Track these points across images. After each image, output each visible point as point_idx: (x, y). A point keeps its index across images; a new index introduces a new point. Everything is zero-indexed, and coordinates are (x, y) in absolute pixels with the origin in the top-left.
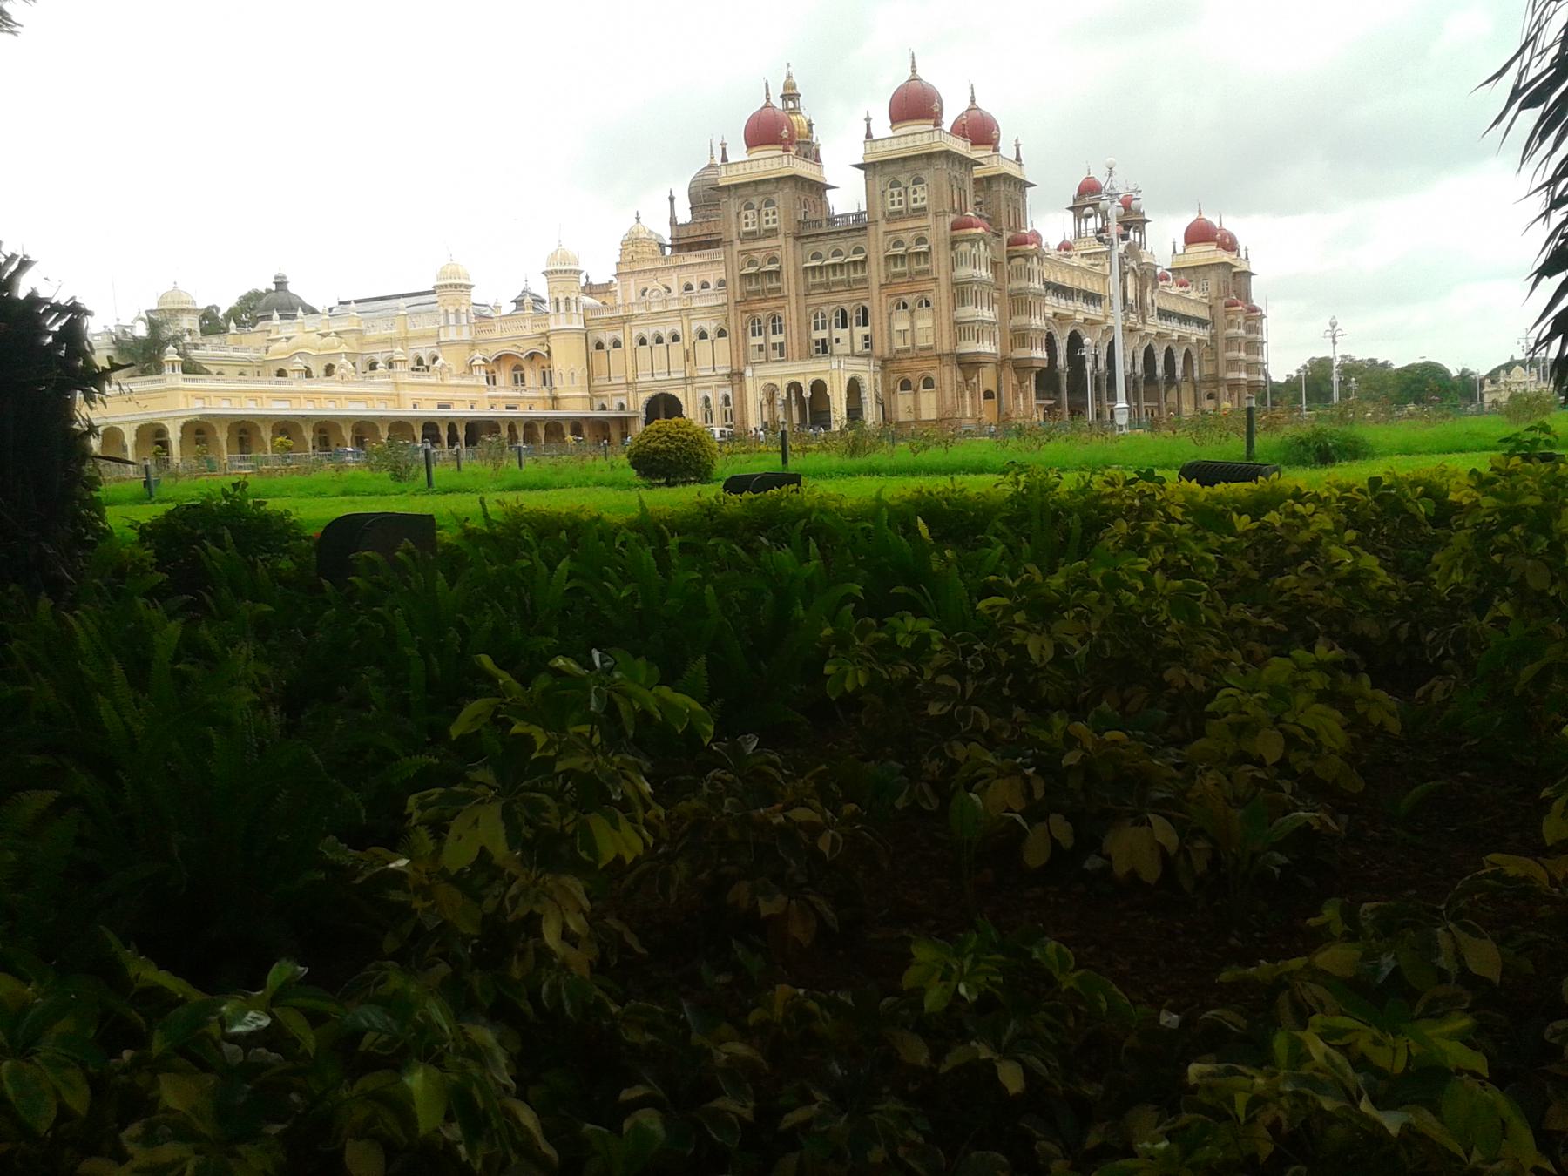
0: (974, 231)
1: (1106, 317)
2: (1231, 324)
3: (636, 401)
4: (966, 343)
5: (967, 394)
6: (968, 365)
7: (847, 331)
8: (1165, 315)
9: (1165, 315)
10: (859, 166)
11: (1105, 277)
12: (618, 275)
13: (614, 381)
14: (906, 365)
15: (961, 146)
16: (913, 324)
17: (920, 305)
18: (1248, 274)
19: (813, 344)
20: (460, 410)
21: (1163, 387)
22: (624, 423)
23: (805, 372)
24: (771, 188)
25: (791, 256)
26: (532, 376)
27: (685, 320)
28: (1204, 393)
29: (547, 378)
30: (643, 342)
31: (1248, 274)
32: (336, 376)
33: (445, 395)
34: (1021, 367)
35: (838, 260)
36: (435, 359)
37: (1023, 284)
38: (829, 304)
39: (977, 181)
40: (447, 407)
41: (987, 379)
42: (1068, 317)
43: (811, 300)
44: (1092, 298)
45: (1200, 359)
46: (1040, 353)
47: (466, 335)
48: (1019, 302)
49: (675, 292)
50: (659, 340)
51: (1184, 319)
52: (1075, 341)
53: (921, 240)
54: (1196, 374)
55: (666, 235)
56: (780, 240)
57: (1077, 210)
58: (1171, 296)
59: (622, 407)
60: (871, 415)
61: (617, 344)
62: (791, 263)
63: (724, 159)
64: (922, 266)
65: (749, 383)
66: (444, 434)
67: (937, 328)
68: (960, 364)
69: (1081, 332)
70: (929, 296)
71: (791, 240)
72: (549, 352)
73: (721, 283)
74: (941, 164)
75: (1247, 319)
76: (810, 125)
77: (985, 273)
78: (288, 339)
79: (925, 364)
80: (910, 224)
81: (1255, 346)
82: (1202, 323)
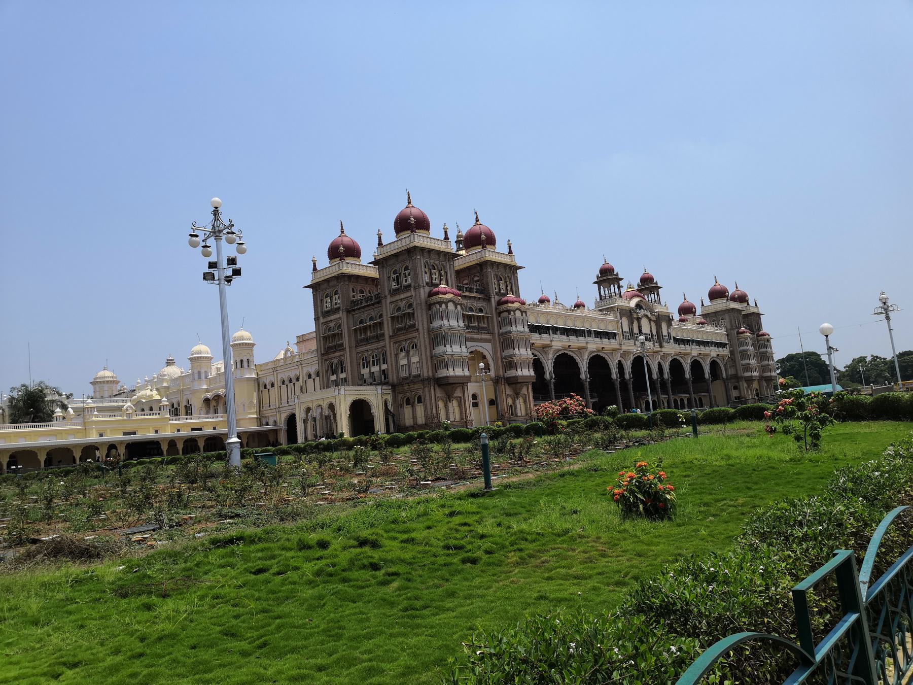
0: (441, 296)
1: (620, 345)
2: (741, 344)
5: (450, 405)
6: (449, 387)
9: (678, 341)
16: (409, 362)
18: (759, 315)
22: (275, 432)
28: (731, 386)
31: (759, 315)
45: (725, 366)
54: (724, 375)
59: (275, 423)
61: (273, 385)
62: (346, 327)
67: (421, 362)
68: (439, 386)
71: (345, 313)
80: (402, 296)
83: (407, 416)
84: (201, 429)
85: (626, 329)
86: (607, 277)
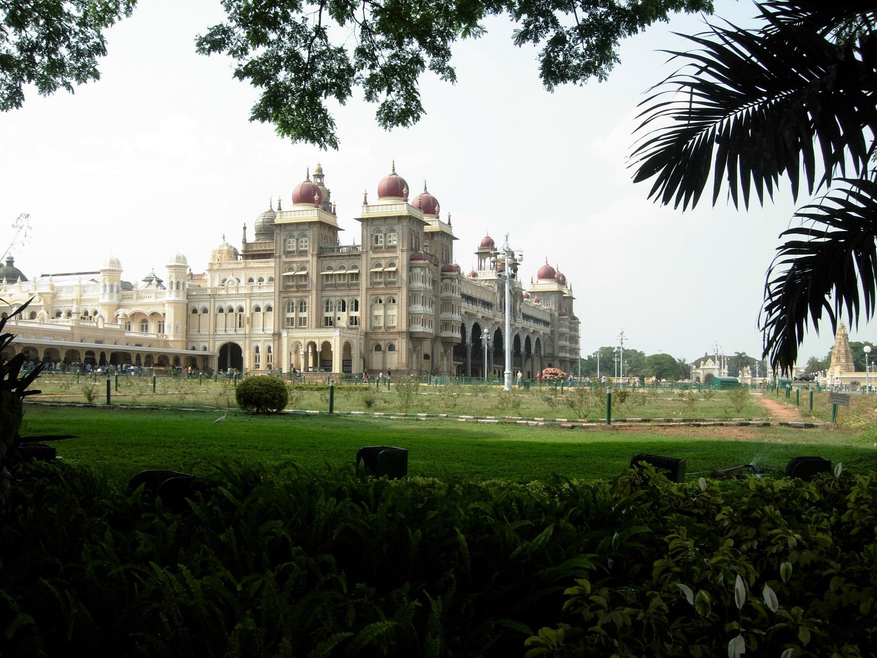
0: (422, 262)
1: (494, 316)
2: (560, 326)
3: (214, 345)
4: (416, 326)
7: (345, 313)
8: (526, 317)
9: (526, 317)
10: (359, 220)
11: (494, 294)
12: (210, 270)
13: (201, 332)
14: (380, 336)
15: (418, 214)
16: (385, 313)
17: (390, 302)
19: (323, 319)
20: (108, 346)
21: (524, 358)
22: (206, 358)
23: (319, 336)
24: (306, 227)
25: (315, 266)
26: (153, 327)
27: (248, 300)
29: (161, 328)
30: (221, 311)
31: (571, 298)
32: (36, 320)
33: (99, 335)
34: (446, 342)
35: (343, 272)
36: (96, 313)
37: (448, 294)
38: (336, 296)
39: (426, 233)
40: (101, 342)
41: (426, 348)
42: (473, 315)
43: (326, 294)
44: (487, 305)
46: (457, 335)
47: (115, 300)
48: (446, 304)
49: (243, 283)
50: (231, 310)
51: (537, 320)
52: (477, 330)
53: (392, 265)
54: (542, 353)
55: (240, 249)
56: (309, 258)
57: (482, 255)
58: (531, 305)
59: (205, 349)
60: (356, 367)
61: (205, 311)
62: (315, 270)
63: (280, 209)
64: (392, 279)
65: (285, 341)
66: (98, 358)
69: (480, 323)
70: (396, 298)
71: (315, 258)
72: (164, 314)
73: (271, 279)
74: (405, 223)
75: (570, 323)
76: (329, 193)
77: (429, 286)
78: (10, 295)
79: (391, 337)
80: (386, 255)
81: (574, 339)
82: (546, 324)
83: (374, 360)
84: (140, 345)
85: (498, 302)
86: (487, 248)
